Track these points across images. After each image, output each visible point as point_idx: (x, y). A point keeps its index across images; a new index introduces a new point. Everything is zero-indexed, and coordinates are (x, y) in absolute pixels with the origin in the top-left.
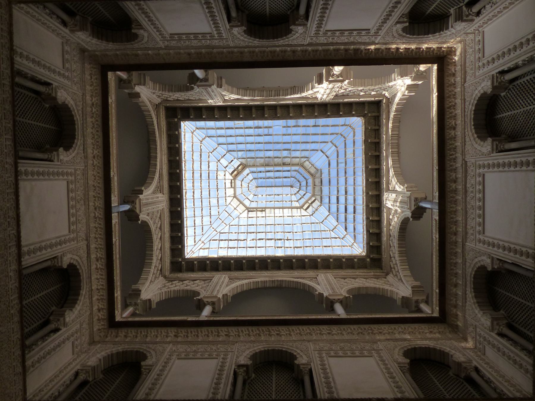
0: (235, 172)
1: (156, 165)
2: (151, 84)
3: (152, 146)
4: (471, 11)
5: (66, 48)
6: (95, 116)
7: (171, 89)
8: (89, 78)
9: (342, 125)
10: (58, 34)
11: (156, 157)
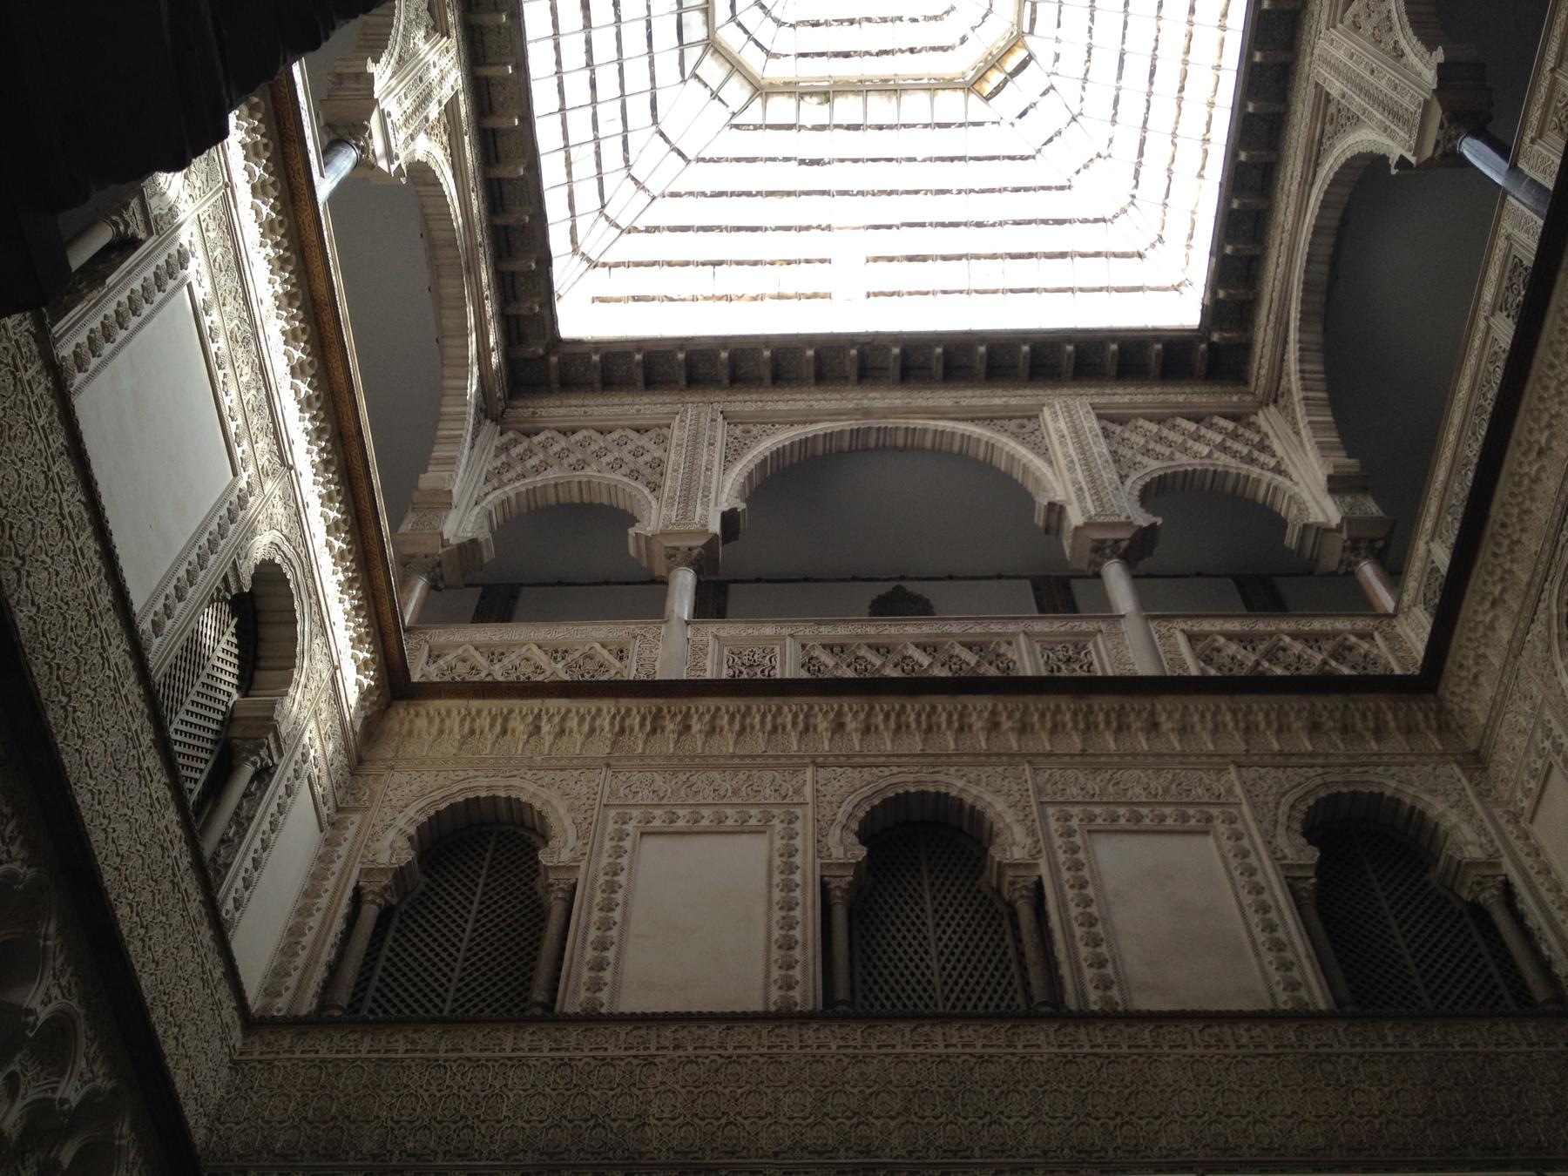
0: (1011, 63)
1: (1324, 205)
2: (1282, 506)
3: (1324, 268)
4: (379, 906)
5: (1526, 804)
6: (1499, 571)
7: (1219, 476)
8: (1483, 679)
9: (617, 265)
10: (1536, 852)
11: (1317, 231)
